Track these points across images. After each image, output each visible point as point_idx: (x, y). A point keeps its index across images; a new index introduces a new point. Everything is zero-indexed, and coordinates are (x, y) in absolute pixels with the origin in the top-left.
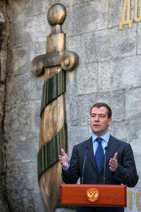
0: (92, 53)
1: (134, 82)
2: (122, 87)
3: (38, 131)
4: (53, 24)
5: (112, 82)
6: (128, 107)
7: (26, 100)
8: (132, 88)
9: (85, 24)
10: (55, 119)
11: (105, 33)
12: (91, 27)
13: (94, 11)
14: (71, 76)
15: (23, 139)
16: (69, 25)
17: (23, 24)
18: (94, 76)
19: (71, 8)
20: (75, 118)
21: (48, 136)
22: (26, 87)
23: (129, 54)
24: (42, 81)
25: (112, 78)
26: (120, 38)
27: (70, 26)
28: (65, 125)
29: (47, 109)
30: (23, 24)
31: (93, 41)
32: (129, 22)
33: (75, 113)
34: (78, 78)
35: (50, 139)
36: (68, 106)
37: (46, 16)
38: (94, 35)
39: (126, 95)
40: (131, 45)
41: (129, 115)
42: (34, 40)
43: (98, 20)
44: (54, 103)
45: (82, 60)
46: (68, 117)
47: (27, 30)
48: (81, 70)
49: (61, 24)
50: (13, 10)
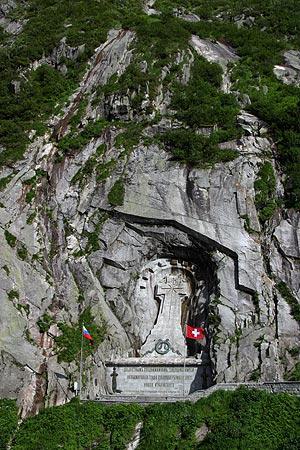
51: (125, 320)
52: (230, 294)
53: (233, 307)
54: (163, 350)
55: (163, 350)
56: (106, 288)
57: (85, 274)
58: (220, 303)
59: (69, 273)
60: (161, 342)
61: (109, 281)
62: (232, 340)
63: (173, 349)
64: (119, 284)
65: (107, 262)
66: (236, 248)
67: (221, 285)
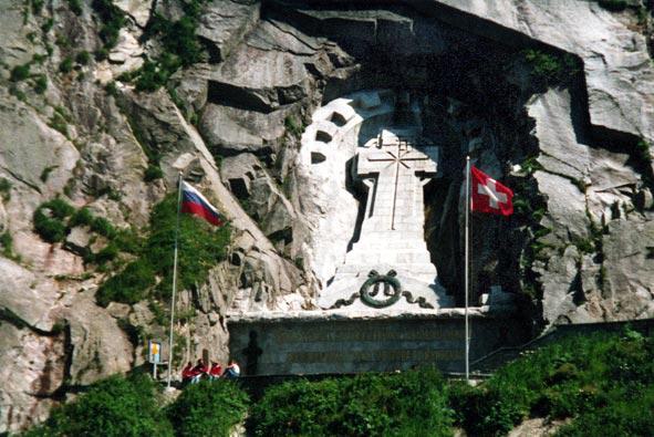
51: (276, 226)
52: (565, 148)
53: (578, 176)
54: (381, 297)
55: (381, 297)
56: (221, 152)
57: (162, 117)
58: (540, 168)
59: (117, 115)
60: (374, 278)
61: (231, 135)
62: (583, 248)
64: (257, 142)
65: (223, 94)
66: (576, 44)
67: (539, 131)
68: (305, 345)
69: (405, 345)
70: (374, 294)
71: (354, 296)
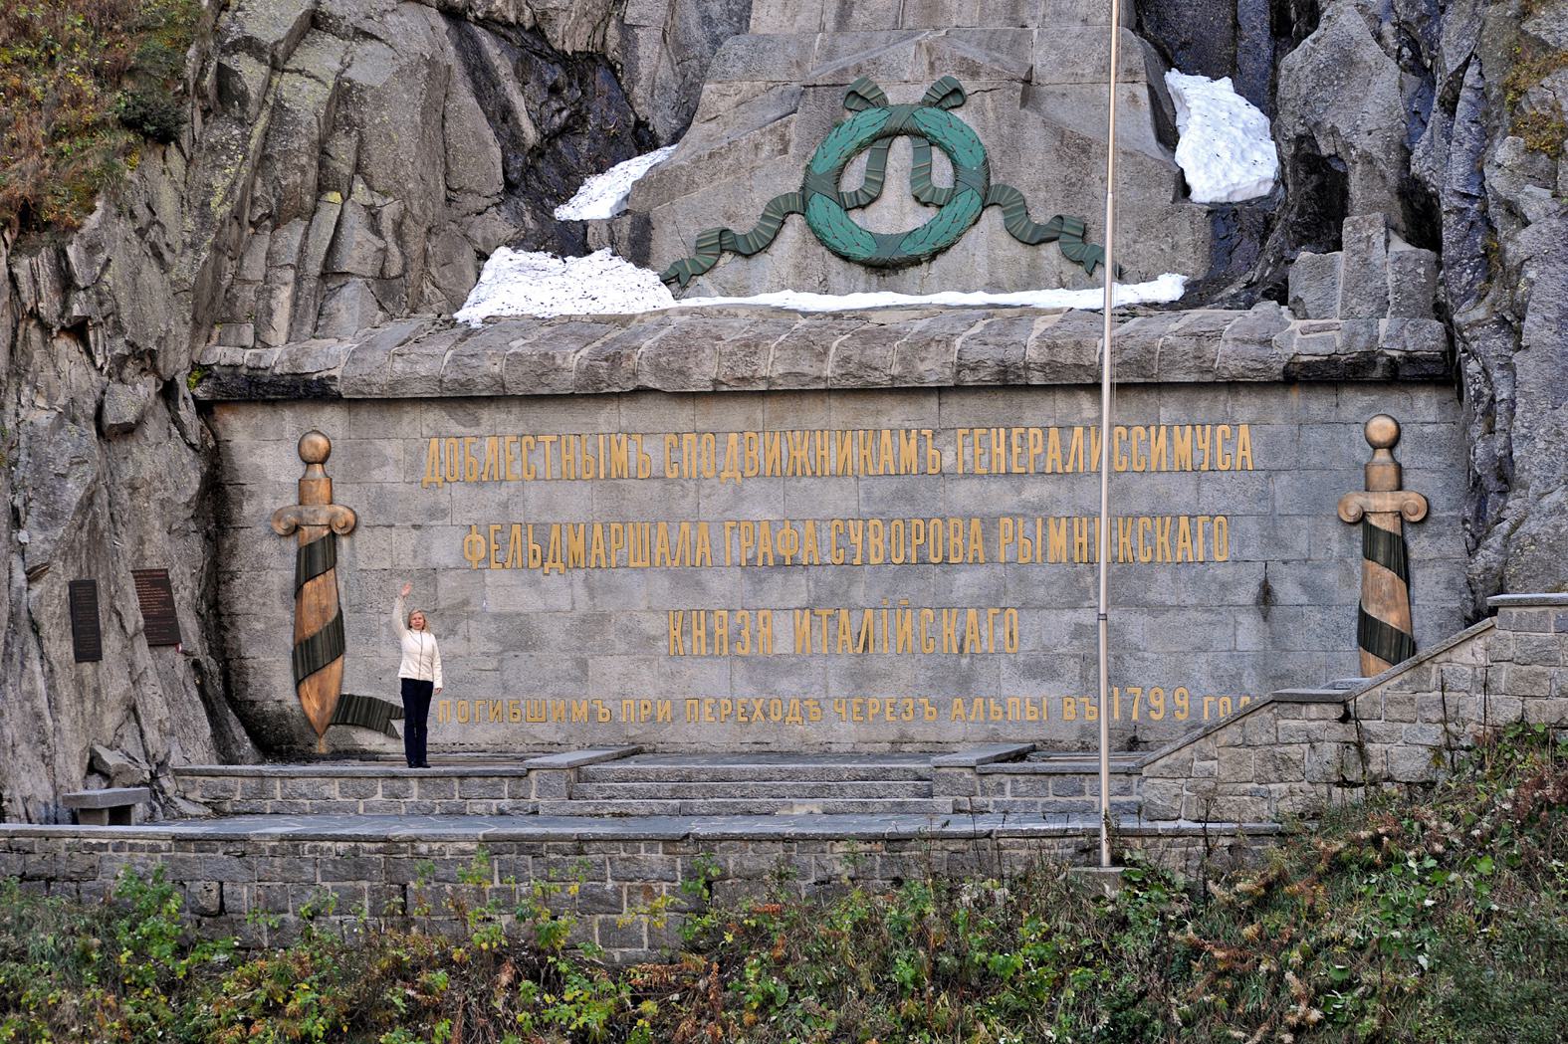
0: (380, 512)
1: (450, 562)
2: (430, 565)
3: (288, 617)
4: (308, 463)
5: (415, 557)
6: (441, 593)
7: (260, 567)
8: (446, 569)
9: (366, 469)
10: (324, 602)
11: (401, 488)
12: (377, 475)
13: (380, 454)
14: (344, 542)
15: (259, 626)
16: (336, 463)
17: (245, 449)
18: (385, 545)
19: (338, 442)
20: (356, 601)
21: (313, 625)
22: (258, 548)
23: (440, 522)
24: (292, 546)
25: (415, 552)
26: (425, 500)
27: (339, 466)
28: (340, 611)
29: (308, 586)
30: (245, 449)
31: (380, 495)
32: (440, 480)
33: (357, 594)
34: (357, 544)
35: (316, 630)
36: (341, 584)
37: (293, 446)
38: (382, 488)
39: (439, 577)
40: (443, 511)
41: (443, 604)
42: (270, 477)
43: (387, 468)
44: (319, 579)
45: (364, 521)
46: (343, 600)
47: (256, 460)
48: (358, 533)
49: (323, 462)
50: (224, 425)
63: (1015, 209)
68: (533, 492)
69: (963, 494)
70: (867, 200)
71: (778, 214)
